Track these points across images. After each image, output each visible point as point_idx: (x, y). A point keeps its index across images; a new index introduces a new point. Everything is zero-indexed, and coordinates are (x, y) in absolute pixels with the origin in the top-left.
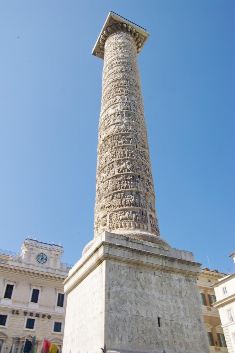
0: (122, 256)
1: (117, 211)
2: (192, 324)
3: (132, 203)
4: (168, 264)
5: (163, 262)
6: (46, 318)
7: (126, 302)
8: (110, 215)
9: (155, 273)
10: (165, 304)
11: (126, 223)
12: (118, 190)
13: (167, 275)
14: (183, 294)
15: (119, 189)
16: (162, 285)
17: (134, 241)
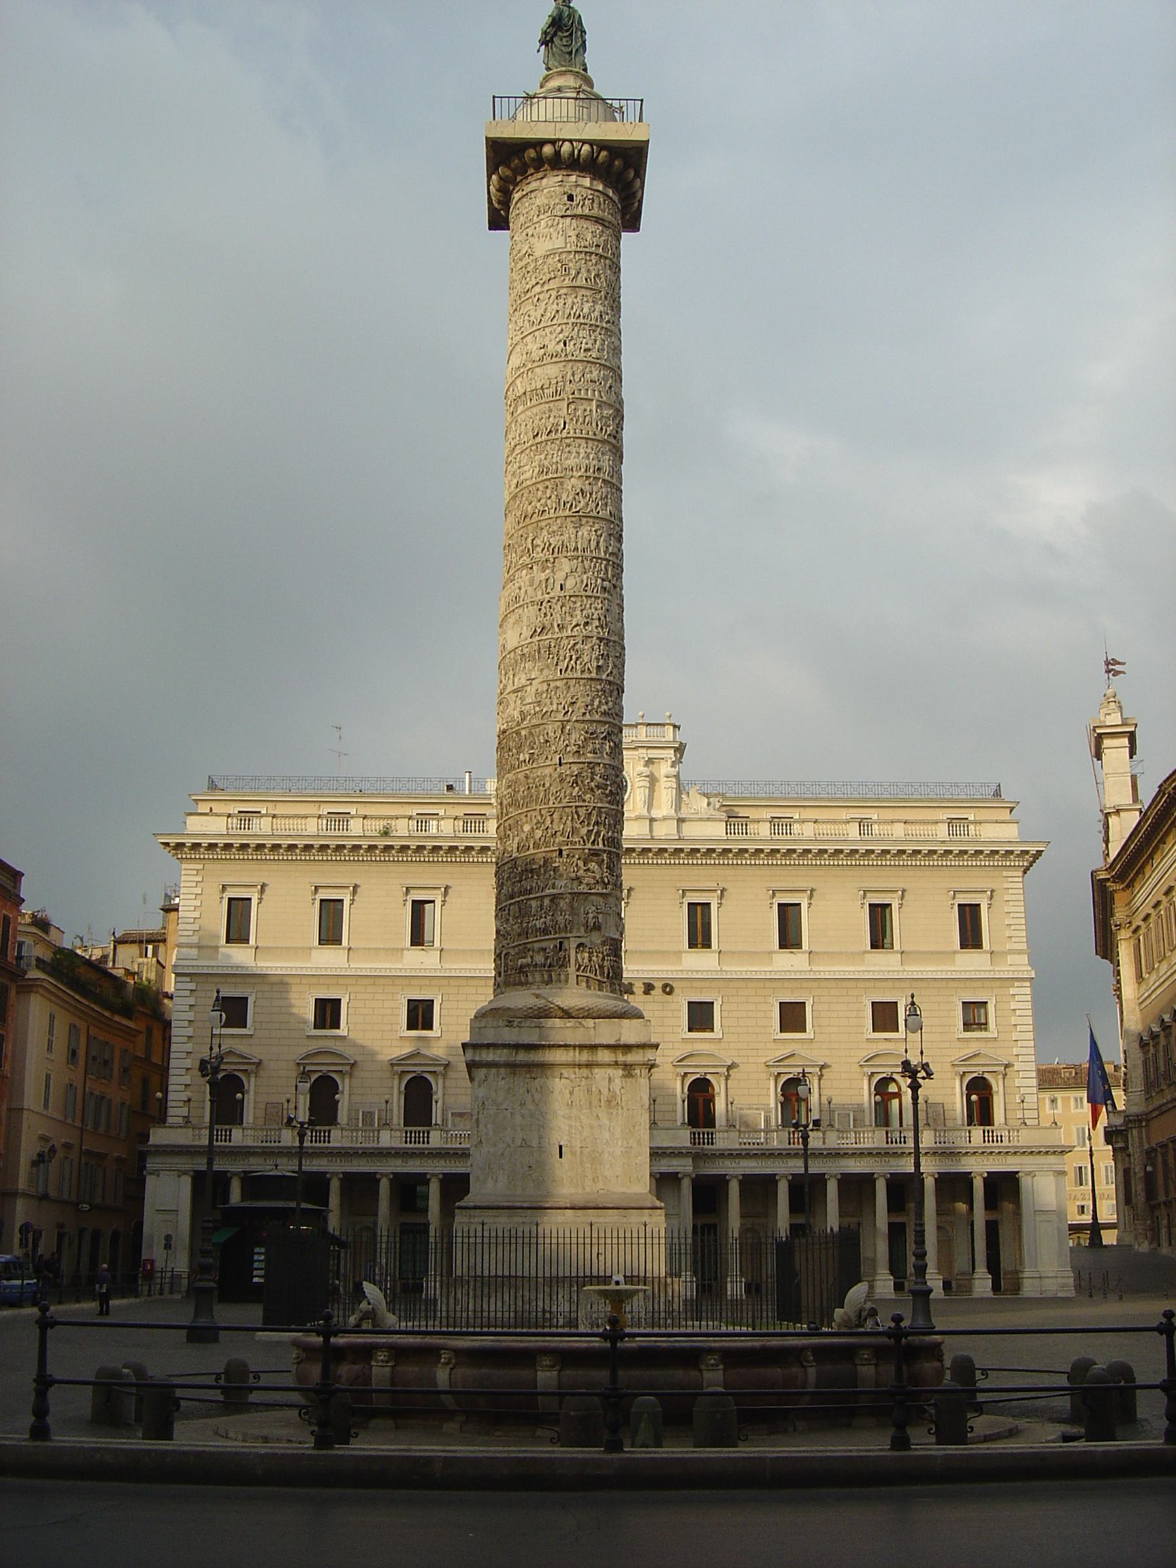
1: (514, 947)
2: (622, 1149)
3: (540, 928)
4: (585, 1057)
5: (575, 1055)
6: (658, 991)
7: (506, 1129)
8: (506, 954)
9: (561, 1074)
10: (573, 1124)
11: (527, 976)
12: (517, 899)
13: (585, 1072)
14: (614, 1103)
15: (519, 897)
16: (571, 1093)
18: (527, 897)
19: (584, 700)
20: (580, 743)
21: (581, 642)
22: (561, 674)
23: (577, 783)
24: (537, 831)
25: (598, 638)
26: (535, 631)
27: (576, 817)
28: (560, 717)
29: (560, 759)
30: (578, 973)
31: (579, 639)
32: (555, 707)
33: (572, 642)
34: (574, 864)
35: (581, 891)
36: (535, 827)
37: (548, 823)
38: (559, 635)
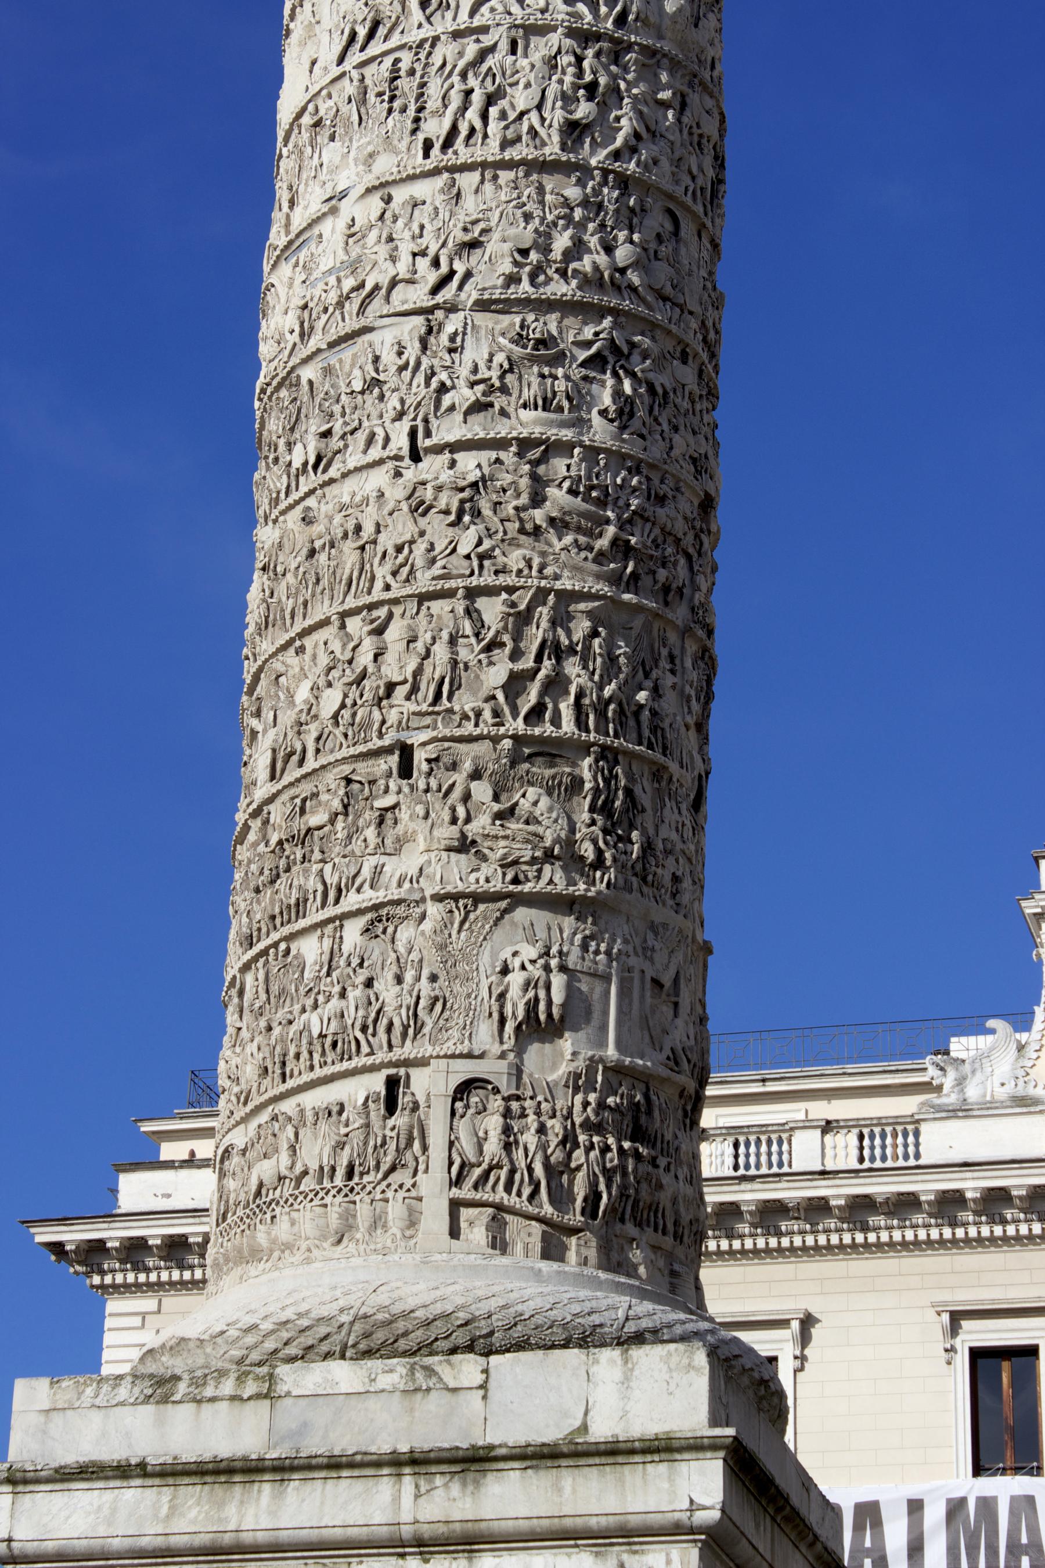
0: (102, 1531)
5: (397, 1499)
17: (209, 1392)
18: (286, 930)
19: (512, 231)
21: (504, 46)
22: (426, 155)
23: (477, 514)
24: (329, 691)
25: (571, 33)
26: (353, 36)
28: (418, 296)
29: (413, 434)
30: (455, 1192)
31: (499, 36)
32: (402, 268)
33: (471, 50)
36: (321, 682)
37: (365, 658)
38: (427, 32)
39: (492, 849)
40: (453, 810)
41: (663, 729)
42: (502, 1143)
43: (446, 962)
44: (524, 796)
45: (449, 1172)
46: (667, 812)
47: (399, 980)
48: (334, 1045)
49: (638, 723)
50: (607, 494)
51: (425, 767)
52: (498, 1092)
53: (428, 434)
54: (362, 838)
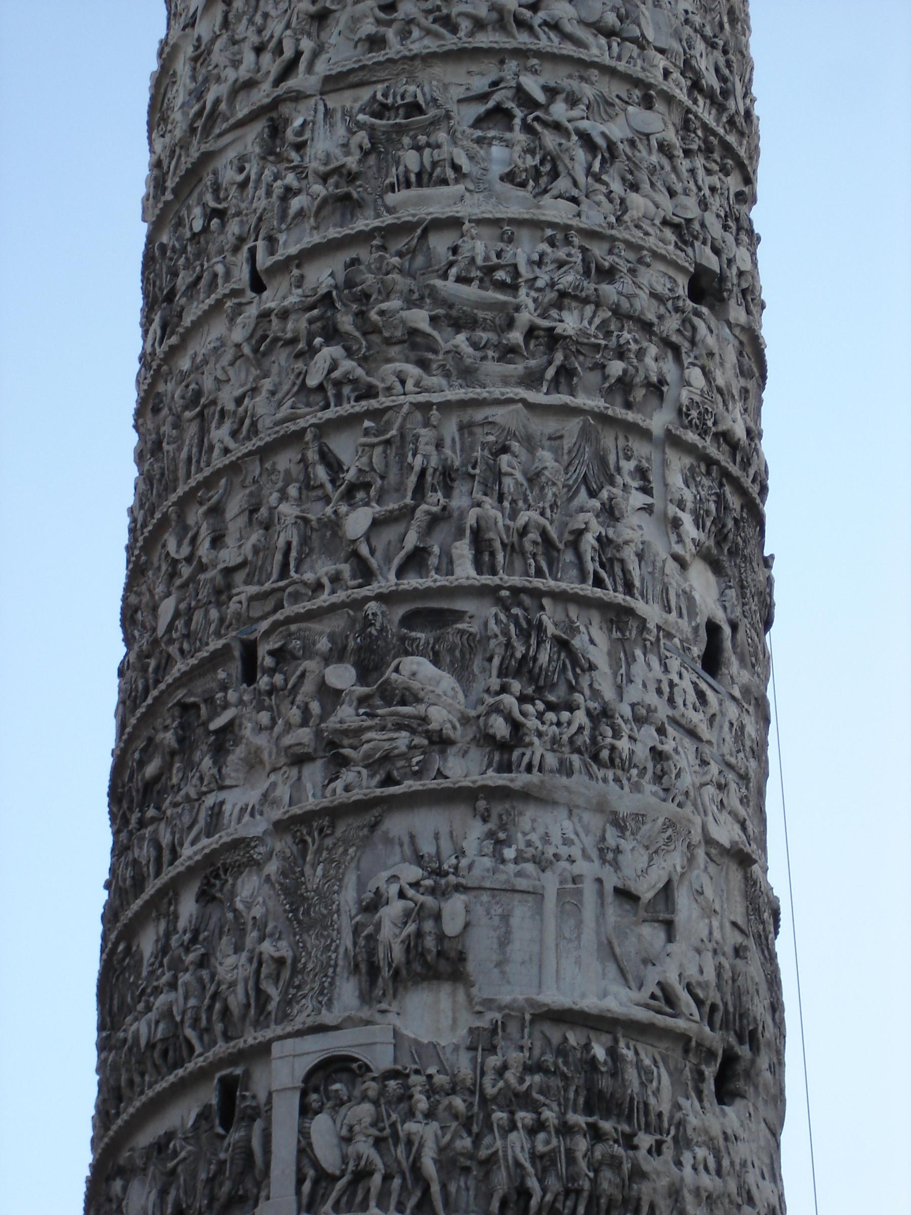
20: (352, 162)
27: (321, 473)
34: (308, 687)
35: (342, 797)
39: (354, 748)
40: (306, 711)
41: (622, 561)
42: (371, 1141)
43: (297, 910)
44: (397, 670)
45: (298, 1192)
46: (639, 669)
47: (238, 949)
48: (165, 1054)
49: (579, 556)
50: (516, 274)
51: (269, 662)
52: (368, 1069)
53: (272, 252)
54: (198, 774)
